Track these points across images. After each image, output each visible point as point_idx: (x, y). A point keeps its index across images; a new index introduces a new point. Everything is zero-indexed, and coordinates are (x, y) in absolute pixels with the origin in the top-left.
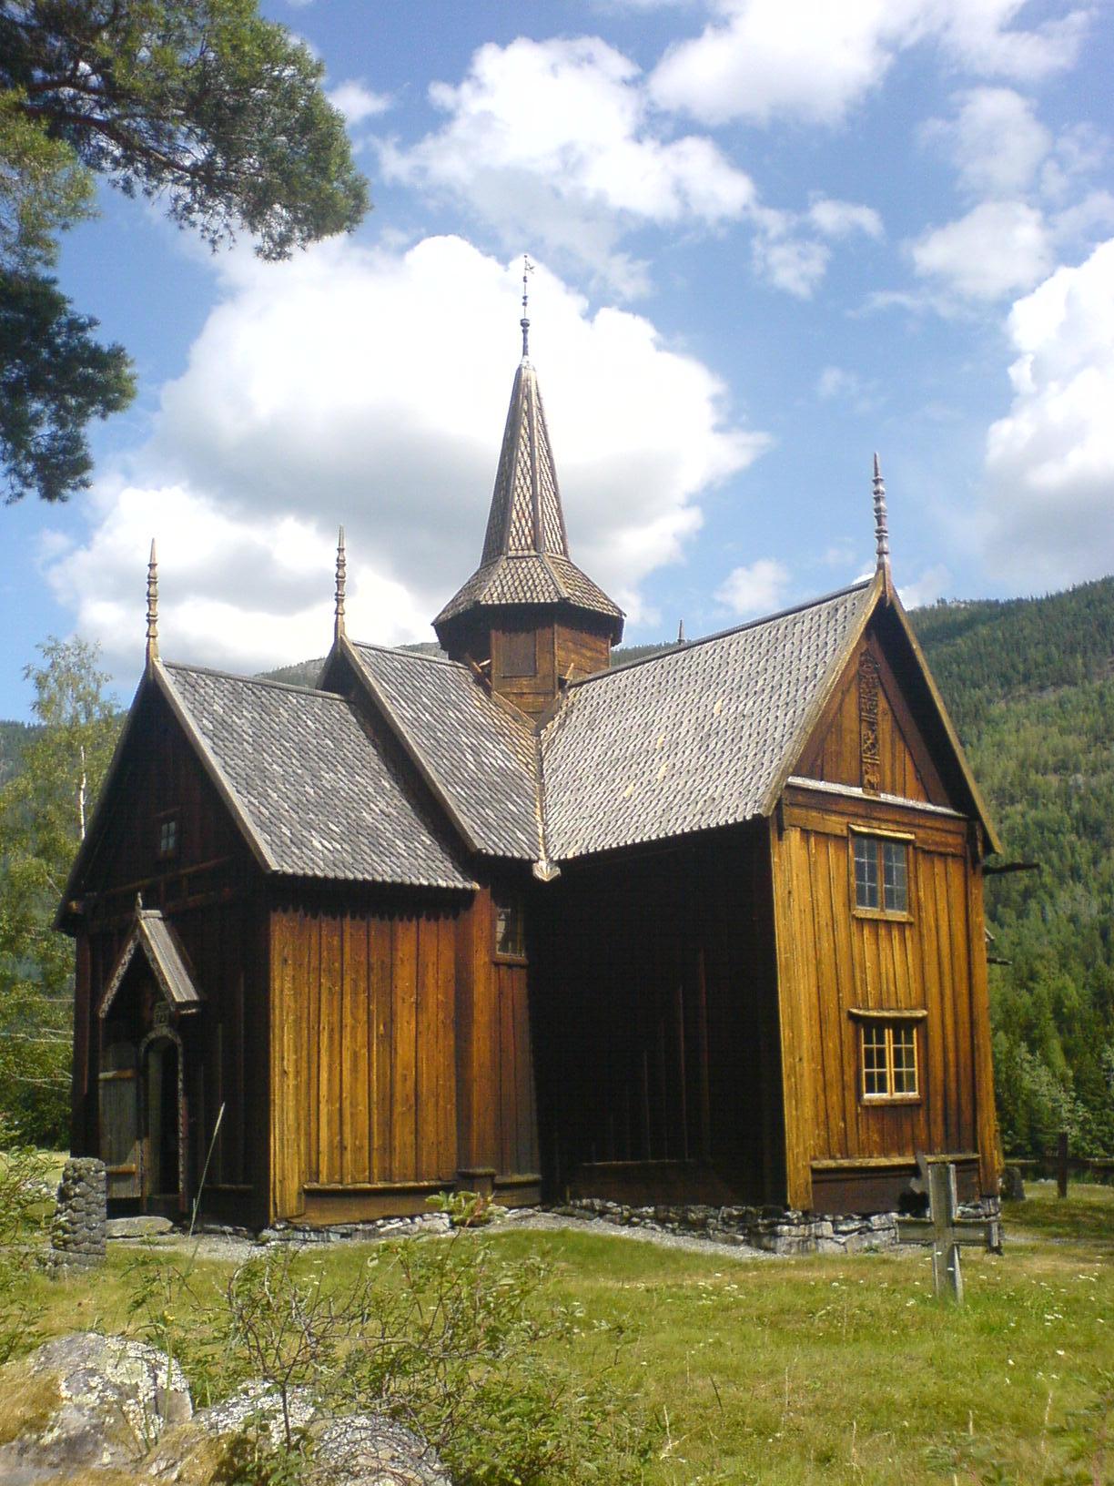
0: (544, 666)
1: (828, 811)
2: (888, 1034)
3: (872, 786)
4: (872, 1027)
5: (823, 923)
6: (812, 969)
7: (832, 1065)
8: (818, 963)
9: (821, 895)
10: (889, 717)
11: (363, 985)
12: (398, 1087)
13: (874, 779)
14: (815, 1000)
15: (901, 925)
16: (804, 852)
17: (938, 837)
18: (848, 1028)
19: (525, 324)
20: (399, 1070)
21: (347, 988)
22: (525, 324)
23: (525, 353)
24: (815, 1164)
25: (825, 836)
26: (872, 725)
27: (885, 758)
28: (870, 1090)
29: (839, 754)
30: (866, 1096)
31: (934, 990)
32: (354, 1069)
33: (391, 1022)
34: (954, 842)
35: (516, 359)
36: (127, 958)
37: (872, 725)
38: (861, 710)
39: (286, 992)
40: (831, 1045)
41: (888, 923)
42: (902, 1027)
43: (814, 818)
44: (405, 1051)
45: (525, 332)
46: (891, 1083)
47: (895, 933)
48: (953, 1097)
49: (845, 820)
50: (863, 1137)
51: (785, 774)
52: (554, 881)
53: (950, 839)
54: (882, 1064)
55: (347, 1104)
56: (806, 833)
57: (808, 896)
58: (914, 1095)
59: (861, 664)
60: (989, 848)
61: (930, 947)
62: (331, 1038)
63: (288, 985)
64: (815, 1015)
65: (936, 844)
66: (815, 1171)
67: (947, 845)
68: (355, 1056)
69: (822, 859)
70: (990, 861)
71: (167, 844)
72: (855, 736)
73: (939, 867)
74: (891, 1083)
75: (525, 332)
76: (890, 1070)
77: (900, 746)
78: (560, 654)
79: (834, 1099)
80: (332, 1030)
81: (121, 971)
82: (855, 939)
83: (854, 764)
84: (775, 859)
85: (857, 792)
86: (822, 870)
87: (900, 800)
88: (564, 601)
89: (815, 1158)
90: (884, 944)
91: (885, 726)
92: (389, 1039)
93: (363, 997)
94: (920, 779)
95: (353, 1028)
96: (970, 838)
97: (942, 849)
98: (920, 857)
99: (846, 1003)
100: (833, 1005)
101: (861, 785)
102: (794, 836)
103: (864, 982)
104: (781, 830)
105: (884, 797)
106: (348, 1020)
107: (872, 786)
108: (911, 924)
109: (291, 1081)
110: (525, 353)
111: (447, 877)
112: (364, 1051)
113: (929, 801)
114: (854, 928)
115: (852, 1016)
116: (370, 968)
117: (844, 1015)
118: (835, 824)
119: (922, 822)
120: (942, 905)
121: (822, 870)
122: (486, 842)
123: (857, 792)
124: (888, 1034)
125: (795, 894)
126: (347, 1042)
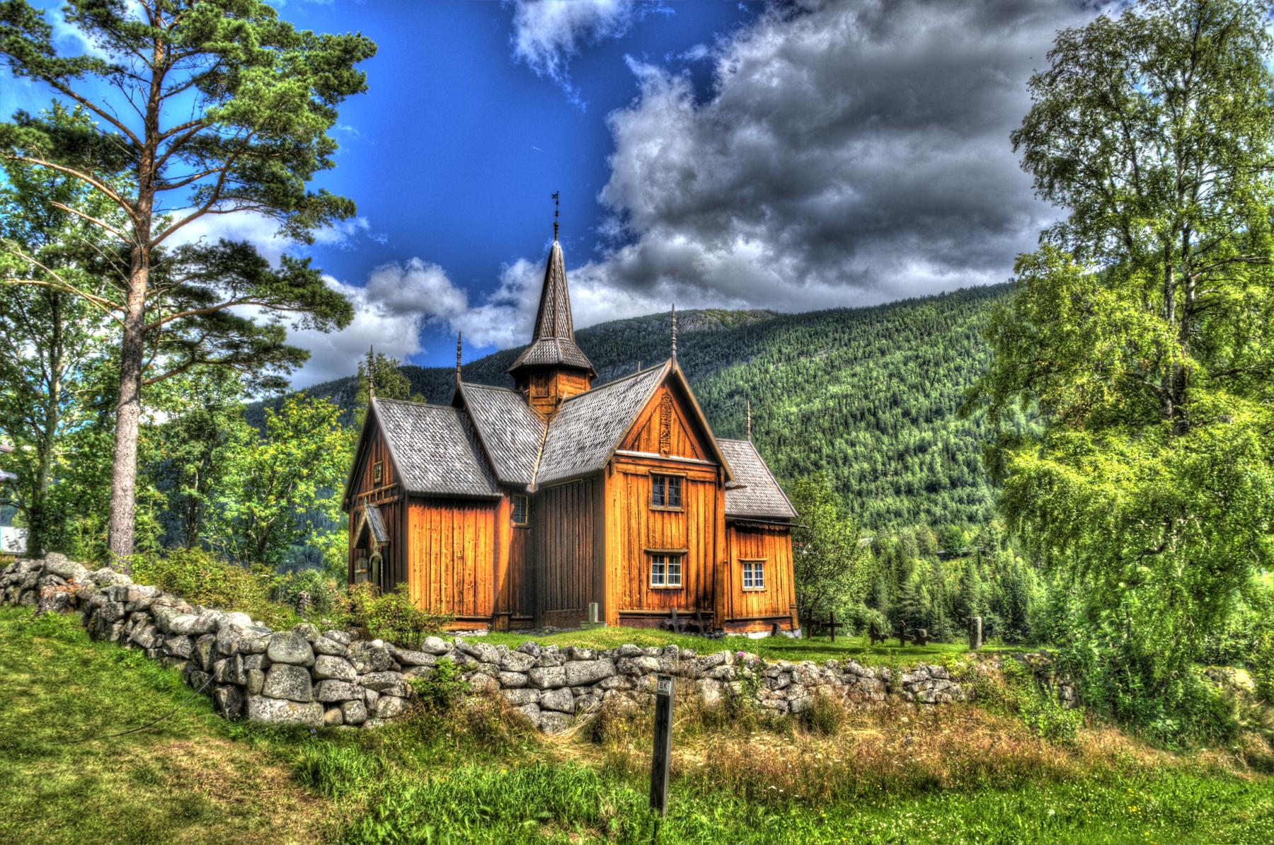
0: (553, 393)
2: (667, 560)
7: (635, 572)
9: (633, 501)
13: (666, 449)
15: (677, 513)
17: (700, 474)
18: (644, 557)
20: (467, 572)
22: (556, 226)
26: (667, 426)
27: (674, 439)
29: (649, 439)
31: (694, 542)
32: (446, 571)
34: (710, 476)
37: (667, 426)
40: (635, 563)
41: (669, 512)
42: (674, 557)
43: (631, 468)
53: (708, 475)
56: (626, 474)
58: (679, 585)
60: (727, 478)
70: (728, 484)
73: (701, 488)
76: (753, 579)
78: (560, 387)
79: (635, 585)
82: (651, 521)
83: (657, 443)
84: (607, 486)
87: (681, 458)
91: (675, 429)
96: (719, 475)
100: (636, 547)
106: (444, 551)
109: (417, 573)
114: (651, 515)
115: (647, 553)
118: (642, 470)
121: (635, 490)
123: (657, 455)
124: (667, 560)
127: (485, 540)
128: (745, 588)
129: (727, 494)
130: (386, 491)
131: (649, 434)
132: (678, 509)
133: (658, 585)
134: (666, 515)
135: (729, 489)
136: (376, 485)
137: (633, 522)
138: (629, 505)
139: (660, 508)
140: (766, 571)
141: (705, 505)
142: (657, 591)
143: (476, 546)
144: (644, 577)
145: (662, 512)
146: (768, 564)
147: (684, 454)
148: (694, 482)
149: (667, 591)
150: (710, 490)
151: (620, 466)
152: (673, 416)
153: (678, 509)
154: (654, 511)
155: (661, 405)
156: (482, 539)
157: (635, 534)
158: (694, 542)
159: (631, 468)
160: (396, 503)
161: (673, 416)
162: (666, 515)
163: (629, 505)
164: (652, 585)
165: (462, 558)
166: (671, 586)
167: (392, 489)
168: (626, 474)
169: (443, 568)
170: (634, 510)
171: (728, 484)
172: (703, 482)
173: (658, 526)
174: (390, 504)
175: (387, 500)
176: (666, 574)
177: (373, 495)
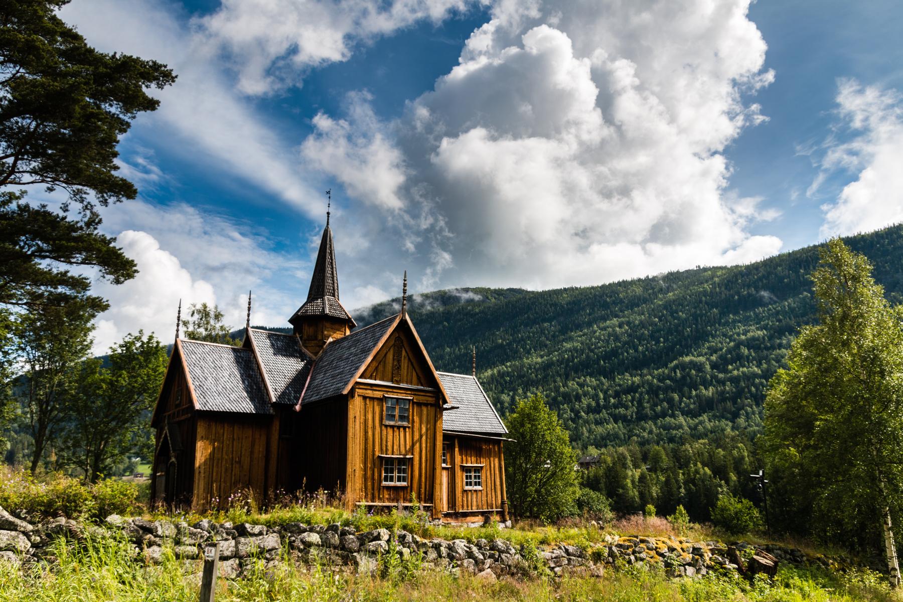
7: (369, 473)
9: (370, 416)
15: (405, 428)
22: (328, 213)
26: (399, 361)
28: (386, 480)
34: (431, 400)
43: (369, 393)
47: (402, 429)
56: (365, 398)
58: (404, 484)
60: (445, 402)
70: (445, 406)
73: (425, 409)
82: (384, 432)
83: (390, 376)
87: (409, 386)
90: (397, 433)
91: (405, 364)
94: (419, 378)
99: (377, 454)
103: (386, 446)
104: (353, 397)
116: (233, 439)
125: (358, 418)
126: (224, 463)
127: (260, 448)
128: (467, 488)
131: (384, 367)
132: (405, 424)
136: (177, 406)
138: (366, 421)
139: (392, 423)
140: (483, 474)
142: (388, 488)
143: (252, 453)
145: (392, 427)
147: (411, 383)
149: (396, 488)
150: (432, 410)
152: (404, 353)
153: (405, 424)
154: (386, 426)
155: (394, 345)
156: (257, 447)
159: (369, 393)
161: (404, 353)
163: (366, 421)
164: (384, 483)
165: (239, 462)
166: (398, 484)
168: (365, 398)
169: (223, 470)
171: (445, 406)
172: (426, 405)
173: (390, 437)
175: (183, 418)
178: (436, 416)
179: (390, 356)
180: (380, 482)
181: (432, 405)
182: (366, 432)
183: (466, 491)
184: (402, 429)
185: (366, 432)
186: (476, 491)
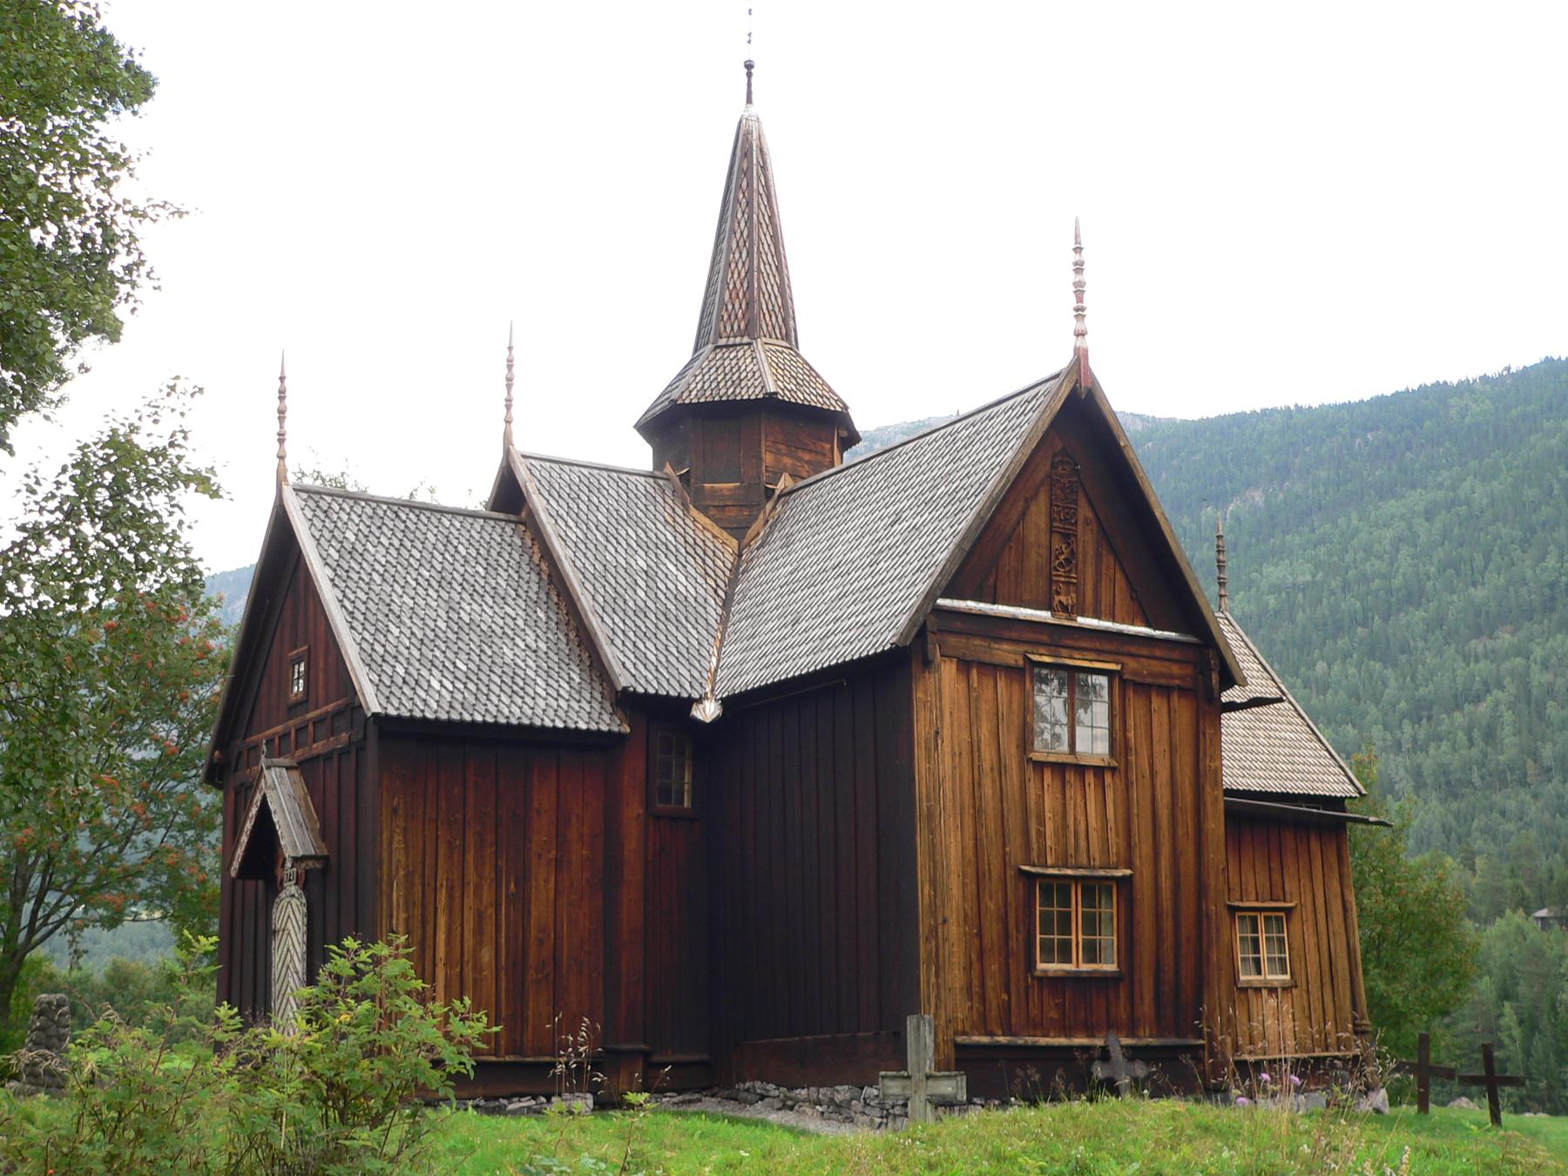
1: (1000, 639)
2: (1076, 896)
3: (1065, 608)
4: (1057, 888)
5: (986, 766)
6: (968, 821)
8: (978, 811)
10: (1095, 526)
11: (490, 838)
12: (532, 950)
14: (970, 854)
16: (962, 686)
17: (1157, 667)
18: (1015, 891)
19: (749, 66)
21: (470, 839)
22: (749, 66)
23: (749, 100)
24: (959, 1039)
25: (991, 668)
26: (1067, 537)
30: (1041, 966)
31: (1144, 849)
33: (523, 880)
35: (736, 109)
36: (254, 811)
37: (1067, 537)
38: (1052, 520)
39: (395, 845)
42: (1092, 888)
43: (976, 647)
44: (540, 910)
45: (749, 75)
46: (1077, 952)
47: (1090, 778)
48: (1169, 975)
49: (1022, 648)
50: (1034, 1011)
51: (931, 595)
52: (717, 722)
53: (1175, 669)
54: (1066, 930)
55: (468, 970)
56: (965, 665)
57: (966, 736)
58: (1111, 967)
59: (1054, 466)
60: (1229, 678)
61: (1140, 795)
62: (450, 897)
63: (398, 838)
64: (971, 871)
65: (1151, 674)
66: (959, 1047)
67: (1172, 677)
68: (480, 917)
69: (988, 693)
70: (1226, 697)
71: (299, 687)
72: (1044, 551)
73: (1157, 702)
74: (1077, 952)
75: (749, 75)
77: (1108, 560)
78: (768, 458)
79: (994, 967)
80: (450, 890)
81: (249, 825)
84: (919, 695)
85: (1044, 615)
86: (986, 708)
88: (772, 397)
89: (964, 1033)
90: (1073, 792)
91: (1087, 539)
92: (522, 901)
93: (489, 851)
95: (478, 887)
96: (1203, 670)
97: (1163, 681)
98: (1130, 693)
100: (996, 863)
101: (1049, 607)
102: (948, 670)
103: (1041, 835)
105: (1084, 621)
106: (471, 877)
107: (1065, 608)
108: (1113, 770)
110: (749, 100)
111: (607, 722)
112: (491, 911)
113: (1149, 625)
117: (1010, 873)
119: (1133, 650)
120: (1161, 748)
121: (986, 708)
122: (624, 680)
123: (1044, 615)
124: (1076, 896)
125: (946, 732)
126: (469, 901)
129: (1228, 719)
130: (317, 722)
133: (1054, 967)
134: (1071, 777)
135: (1233, 707)
137: (988, 791)
138: (974, 749)
141: (1172, 750)
144: (1017, 942)
146: (1296, 917)
148: (1145, 688)
150: (1183, 712)
151: (952, 640)
154: (1040, 766)
157: (991, 823)
158: (1144, 849)
160: (343, 753)
161: (1084, 511)
162: (1071, 777)
163: (974, 749)
167: (337, 714)
170: (988, 755)
171: (1226, 697)
172: (1166, 691)
174: (327, 757)
175: (319, 747)
176: (1077, 937)
177: (284, 736)
178: (1198, 735)
179: (1038, 514)
180: (1030, 964)
181: (1183, 691)
182: (976, 785)
183: (1244, 990)
184: (1090, 778)
185: (976, 785)
186: (1272, 990)
